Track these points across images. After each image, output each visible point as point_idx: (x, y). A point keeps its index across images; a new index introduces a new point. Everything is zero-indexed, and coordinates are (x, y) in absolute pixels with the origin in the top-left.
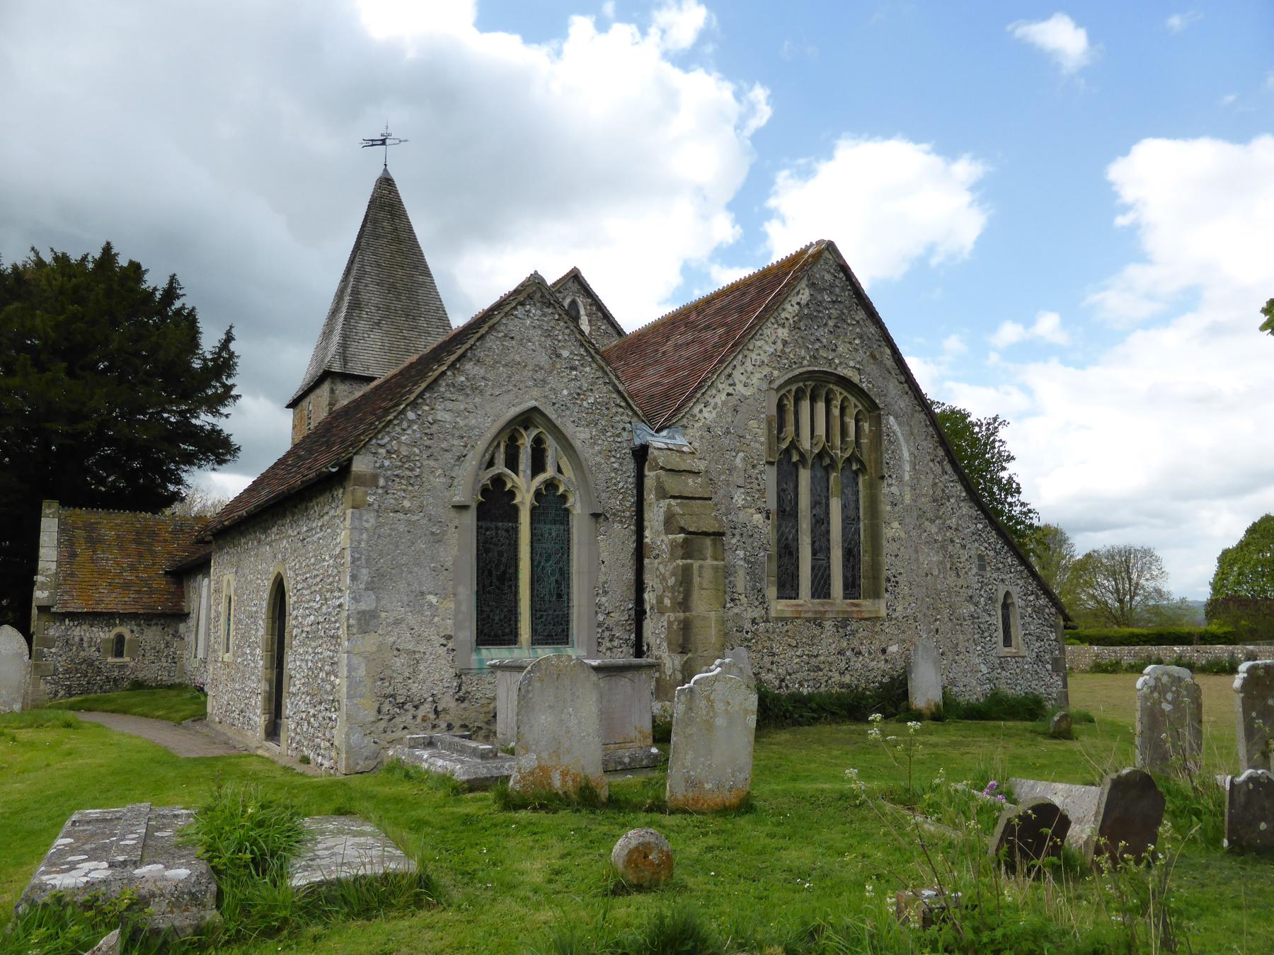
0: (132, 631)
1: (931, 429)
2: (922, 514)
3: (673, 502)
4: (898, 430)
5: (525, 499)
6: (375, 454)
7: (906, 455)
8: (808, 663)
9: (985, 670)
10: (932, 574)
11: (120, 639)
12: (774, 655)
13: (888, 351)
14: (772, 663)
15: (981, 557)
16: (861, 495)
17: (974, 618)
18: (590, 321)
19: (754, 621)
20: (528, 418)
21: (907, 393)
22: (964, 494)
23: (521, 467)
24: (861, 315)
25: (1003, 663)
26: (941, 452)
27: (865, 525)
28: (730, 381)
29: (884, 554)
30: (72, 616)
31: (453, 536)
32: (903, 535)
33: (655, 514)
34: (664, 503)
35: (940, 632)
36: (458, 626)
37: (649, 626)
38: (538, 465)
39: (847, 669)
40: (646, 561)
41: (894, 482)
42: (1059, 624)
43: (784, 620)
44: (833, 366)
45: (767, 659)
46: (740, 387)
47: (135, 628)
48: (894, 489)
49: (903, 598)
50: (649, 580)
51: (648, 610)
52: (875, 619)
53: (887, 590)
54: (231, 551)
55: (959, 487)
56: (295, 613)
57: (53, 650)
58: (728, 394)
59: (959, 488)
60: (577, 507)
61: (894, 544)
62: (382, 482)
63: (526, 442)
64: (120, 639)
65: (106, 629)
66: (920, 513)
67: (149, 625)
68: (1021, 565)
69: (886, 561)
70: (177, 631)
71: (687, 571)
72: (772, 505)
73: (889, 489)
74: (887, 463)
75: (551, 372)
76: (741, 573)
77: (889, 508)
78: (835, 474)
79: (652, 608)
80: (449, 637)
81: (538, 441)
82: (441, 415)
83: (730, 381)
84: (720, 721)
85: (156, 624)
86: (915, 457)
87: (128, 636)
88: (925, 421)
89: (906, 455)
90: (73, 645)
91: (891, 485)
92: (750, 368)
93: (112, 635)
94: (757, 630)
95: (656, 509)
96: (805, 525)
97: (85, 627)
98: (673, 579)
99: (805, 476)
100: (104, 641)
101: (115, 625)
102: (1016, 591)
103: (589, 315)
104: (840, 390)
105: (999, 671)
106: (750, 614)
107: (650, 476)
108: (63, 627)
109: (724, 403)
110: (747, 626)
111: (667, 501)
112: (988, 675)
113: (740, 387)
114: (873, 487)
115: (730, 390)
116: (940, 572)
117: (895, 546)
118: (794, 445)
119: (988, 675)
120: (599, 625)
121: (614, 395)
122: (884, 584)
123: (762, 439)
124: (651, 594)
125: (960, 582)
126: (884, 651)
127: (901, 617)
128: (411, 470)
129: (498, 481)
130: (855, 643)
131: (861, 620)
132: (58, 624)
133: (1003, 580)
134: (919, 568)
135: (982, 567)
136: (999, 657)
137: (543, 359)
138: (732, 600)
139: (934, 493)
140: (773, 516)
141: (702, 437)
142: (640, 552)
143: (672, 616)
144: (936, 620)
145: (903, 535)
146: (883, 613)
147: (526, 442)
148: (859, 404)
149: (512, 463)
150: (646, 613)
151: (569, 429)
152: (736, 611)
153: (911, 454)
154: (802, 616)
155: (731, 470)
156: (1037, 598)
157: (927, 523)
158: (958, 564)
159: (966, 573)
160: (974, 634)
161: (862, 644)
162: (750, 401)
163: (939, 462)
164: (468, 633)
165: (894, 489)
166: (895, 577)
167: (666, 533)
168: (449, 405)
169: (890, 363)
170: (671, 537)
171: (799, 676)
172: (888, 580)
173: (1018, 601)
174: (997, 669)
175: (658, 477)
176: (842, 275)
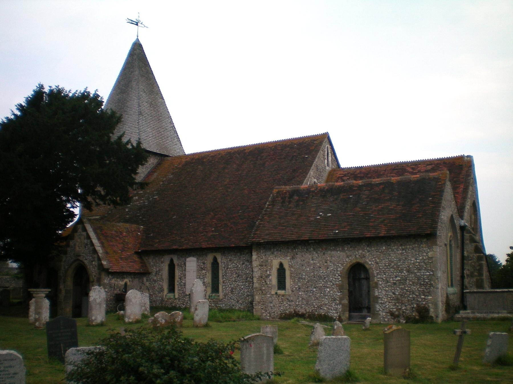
0: (130, 281)
37: (466, 281)
40: (465, 261)
47: (130, 279)
50: (466, 267)
51: (465, 275)
54: (282, 250)
56: (379, 276)
67: (135, 278)
70: (143, 281)
85: (137, 278)
87: (128, 283)
90: (112, 287)
101: (124, 278)
107: (467, 235)
108: (109, 279)
124: (467, 271)
132: (107, 277)
142: (463, 258)
143: (478, 278)
170: (478, 255)
175: (470, 236)
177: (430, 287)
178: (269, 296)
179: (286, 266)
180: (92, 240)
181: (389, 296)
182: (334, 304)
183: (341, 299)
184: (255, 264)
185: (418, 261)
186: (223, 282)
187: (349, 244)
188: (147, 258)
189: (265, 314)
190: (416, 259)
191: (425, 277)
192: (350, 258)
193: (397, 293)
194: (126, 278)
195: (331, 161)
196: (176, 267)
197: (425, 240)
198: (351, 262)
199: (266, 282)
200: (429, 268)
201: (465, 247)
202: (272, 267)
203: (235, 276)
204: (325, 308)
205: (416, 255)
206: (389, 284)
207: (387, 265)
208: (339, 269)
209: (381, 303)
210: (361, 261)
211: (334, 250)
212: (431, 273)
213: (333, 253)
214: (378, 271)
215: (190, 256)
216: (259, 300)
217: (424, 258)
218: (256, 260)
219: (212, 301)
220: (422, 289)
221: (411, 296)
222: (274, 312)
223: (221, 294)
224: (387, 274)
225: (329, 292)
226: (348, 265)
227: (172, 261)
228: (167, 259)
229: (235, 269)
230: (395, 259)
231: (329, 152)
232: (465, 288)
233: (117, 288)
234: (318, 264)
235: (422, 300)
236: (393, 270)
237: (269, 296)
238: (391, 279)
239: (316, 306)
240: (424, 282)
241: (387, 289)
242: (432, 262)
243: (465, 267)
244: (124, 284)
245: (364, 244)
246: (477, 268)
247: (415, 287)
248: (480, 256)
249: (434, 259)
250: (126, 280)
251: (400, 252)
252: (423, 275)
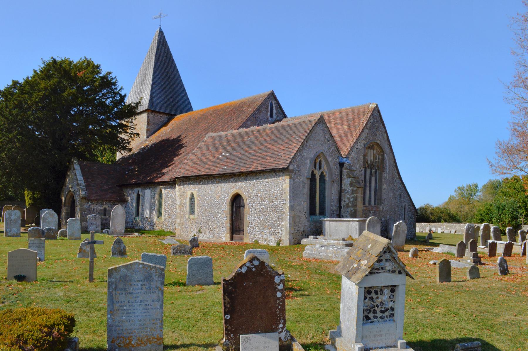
0: (109, 207)
3: (353, 179)
5: (318, 177)
6: (293, 164)
7: (388, 166)
11: (105, 209)
13: (386, 135)
15: (400, 195)
16: (378, 176)
18: (276, 109)
20: (318, 156)
23: (317, 168)
24: (381, 125)
27: (378, 185)
30: (91, 201)
33: (347, 181)
34: (350, 179)
36: (307, 210)
38: (320, 168)
46: (359, 146)
47: (110, 206)
48: (385, 175)
50: (343, 199)
51: (342, 206)
57: (86, 213)
58: (357, 148)
60: (327, 178)
62: (294, 172)
63: (318, 161)
64: (105, 209)
65: (101, 206)
67: (114, 205)
69: (383, 195)
71: (357, 197)
72: (363, 179)
75: (324, 142)
77: (384, 180)
78: (373, 170)
79: (344, 206)
80: (305, 212)
81: (320, 161)
82: (305, 154)
84: (401, 232)
87: (108, 208)
89: (388, 166)
92: (361, 141)
93: (103, 208)
95: (346, 180)
96: (368, 184)
97: (95, 205)
98: (353, 199)
99: (368, 171)
100: (101, 210)
103: (276, 107)
107: (345, 172)
111: (351, 179)
113: (359, 146)
114: (381, 174)
118: (367, 163)
120: (332, 210)
121: (336, 149)
122: (382, 201)
123: (362, 161)
124: (344, 202)
126: (381, 220)
128: (299, 169)
129: (313, 172)
133: (404, 201)
135: (400, 197)
137: (322, 138)
141: (352, 161)
142: (341, 191)
143: (352, 209)
147: (318, 161)
149: (315, 168)
150: (342, 207)
151: (328, 158)
155: (357, 169)
156: (411, 207)
157: (391, 184)
164: (308, 212)
165: (385, 175)
167: (351, 187)
168: (306, 151)
169: (386, 139)
170: (352, 188)
172: (383, 200)
175: (348, 172)
176: (378, 114)
177: (283, 214)
178: (185, 219)
179: (195, 196)
180: (77, 176)
181: (256, 221)
182: (222, 227)
183: (226, 224)
184: (178, 194)
185: (276, 191)
186: (165, 209)
187: (233, 178)
188: (126, 190)
189: (182, 234)
190: (275, 190)
191: (280, 205)
192: (233, 189)
193: (261, 219)
194: (105, 204)
195: (276, 113)
196: (140, 197)
197: (281, 174)
198: (233, 192)
199: (183, 208)
200: (283, 198)
201: (343, 181)
202: (187, 196)
203: (171, 204)
204: (217, 230)
205: (275, 187)
206: (257, 211)
207: (256, 195)
208: (226, 199)
209: (251, 227)
210: (240, 193)
211: (224, 182)
212: (285, 202)
213: (223, 185)
214: (250, 200)
215: (147, 189)
216: (179, 223)
217: (280, 189)
218: (178, 191)
219: (158, 223)
220: (277, 216)
221: (270, 222)
222: (188, 232)
223: (163, 217)
224: (256, 203)
225: (220, 217)
226: (231, 196)
227: (138, 192)
228: (136, 190)
229: (171, 198)
230: (261, 190)
231: (274, 106)
232: (341, 217)
233: (96, 212)
234: (214, 195)
235: (277, 225)
236: (260, 199)
237: (185, 219)
238: (258, 207)
239: (212, 228)
240: (279, 210)
241: (255, 215)
242: (285, 193)
243: (342, 199)
244: (103, 209)
245: (242, 178)
246: (352, 200)
247: (273, 214)
248: (353, 189)
249: (286, 190)
250: (104, 206)
251: (265, 184)
252: (279, 204)
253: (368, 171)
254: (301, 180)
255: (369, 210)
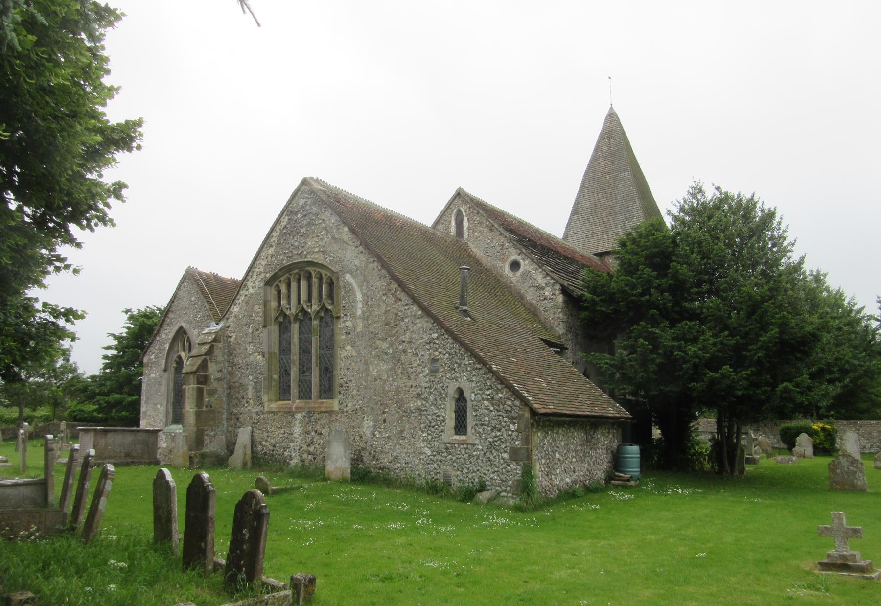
1: (383, 271)
2: (374, 336)
4: (353, 281)
7: (359, 296)
8: (287, 438)
9: (429, 452)
10: (381, 379)
12: (268, 432)
14: (268, 436)
15: (434, 361)
17: (421, 411)
19: (257, 413)
21: (362, 252)
22: (420, 313)
25: (449, 447)
26: (394, 286)
28: (246, 288)
29: (339, 368)
31: (164, 383)
32: (354, 354)
35: (387, 421)
39: (312, 443)
41: (348, 319)
42: (523, 415)
43: (274, 413)
44: (304, 256)
45: (265, 434)
49: (353, 398)
52: (331, 412)
53: (340, 393)
55: (415, 308)
58: (246, 296)
59: (414, 309)
61: (347, 361)
66: (372, 335)
68: (479, 363)
73: (345, 323)
74: (344, 307)
76: (250, 388)
77: (343, 337)
83: (246, 288)
86: (368, 296)
88: (377, 267)
89: (359, 296)
91: (346, 321)
94: (259, 418)
99: (295, 327)
102: (466, 386)
104: (314, 268)
105: (445, 454)
106: (255, 410)
109: (243, 301)
110: (254, 416)
112: (432, 457)
115: (247, 293)
116: (388, 377)
117: (347, 362)
119: (432, 457)
122: (337, 389)
125: (411, 383)
127: (350, 412)
130: (318, 428)
131: (321, 412)
134: (367, 375)
136: (446, 443)
138: (247, 402)
139: (386, 318)
140: (267, 356)
144: (384, 413)
145: (354, 354)
146: (336, 407)
148: (327, 273)
152: (249, 408)
153: (364, 295)
154: (282, 410)
158: (410, 369)
159: (416, 375)
160: (421, 424)
161: (323, 428)
162: (254, 296)
163: (392, 294)
165: (349, 324)
166: (346, 383)
171: (284, 444)
173: (470, 396)
174: (443, 453)
253: (295, 327)
254: (158, 374)
255: (290, 412)
